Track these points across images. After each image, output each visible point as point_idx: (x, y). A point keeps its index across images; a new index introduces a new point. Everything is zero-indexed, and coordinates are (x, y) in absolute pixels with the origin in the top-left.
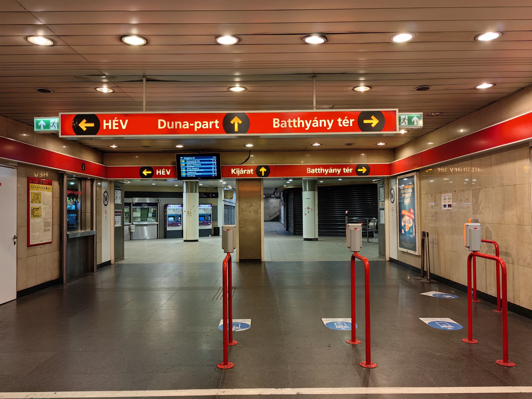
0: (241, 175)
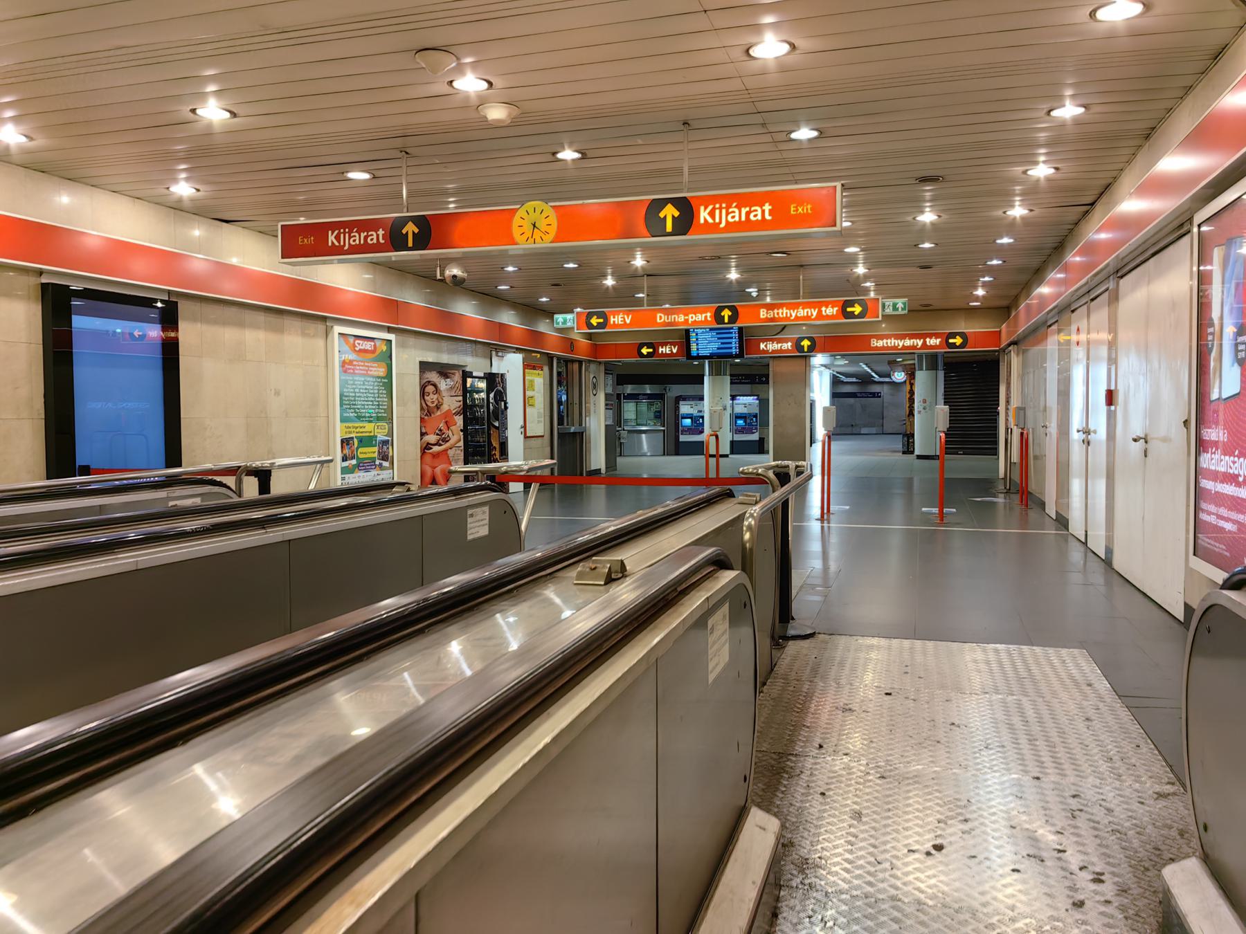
0: (773, 351)
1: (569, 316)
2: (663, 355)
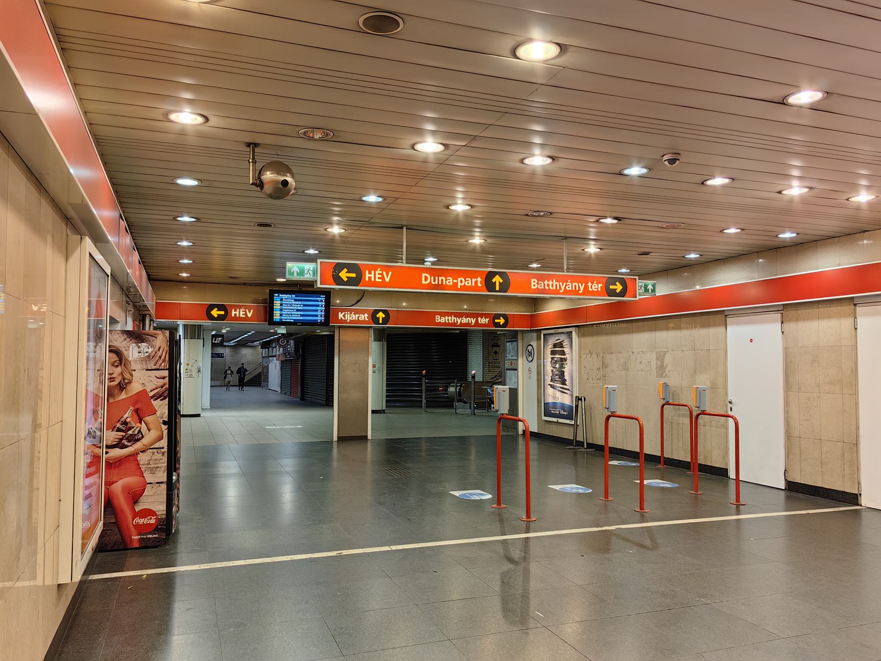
1: (309, 266)
2: (236, 318)
